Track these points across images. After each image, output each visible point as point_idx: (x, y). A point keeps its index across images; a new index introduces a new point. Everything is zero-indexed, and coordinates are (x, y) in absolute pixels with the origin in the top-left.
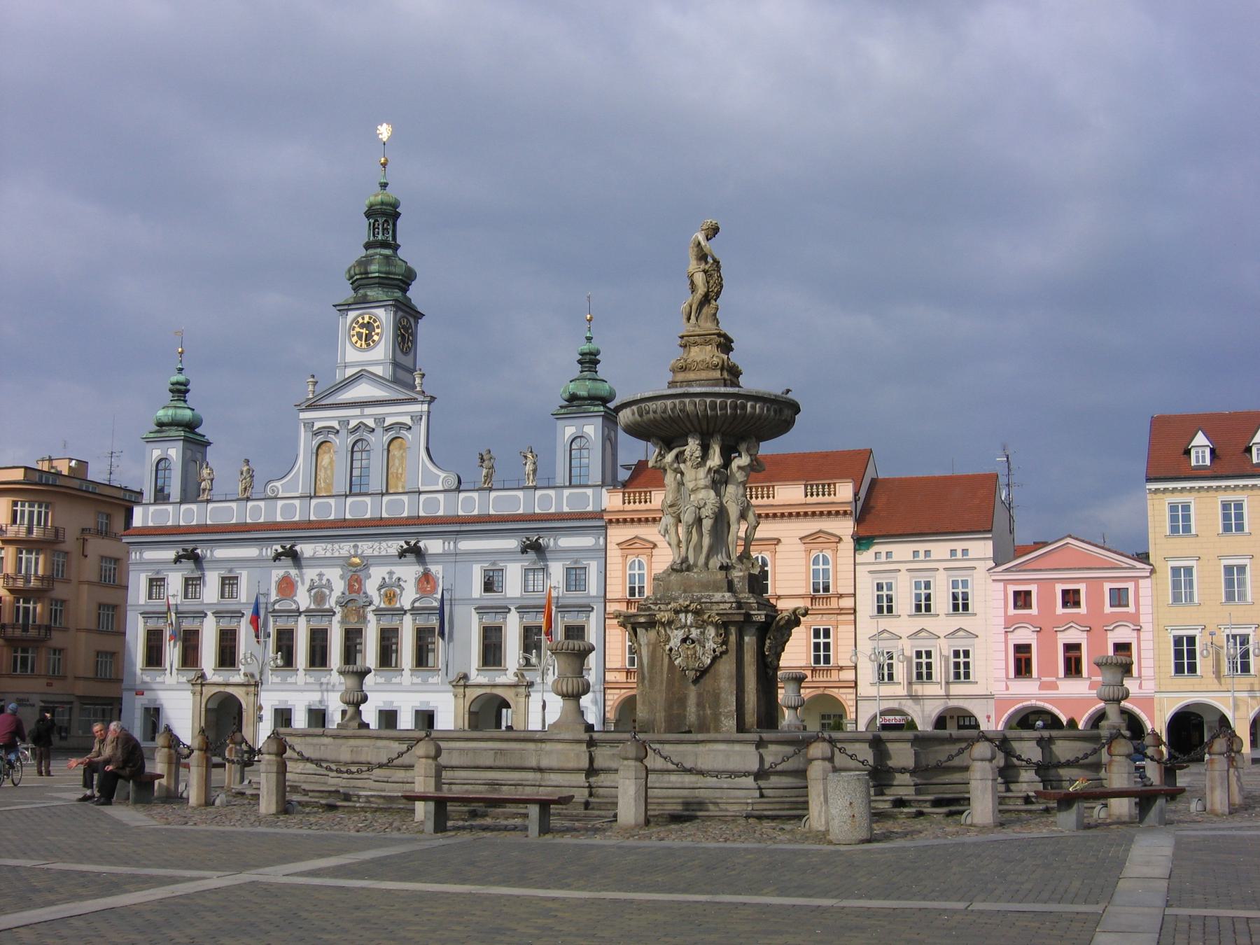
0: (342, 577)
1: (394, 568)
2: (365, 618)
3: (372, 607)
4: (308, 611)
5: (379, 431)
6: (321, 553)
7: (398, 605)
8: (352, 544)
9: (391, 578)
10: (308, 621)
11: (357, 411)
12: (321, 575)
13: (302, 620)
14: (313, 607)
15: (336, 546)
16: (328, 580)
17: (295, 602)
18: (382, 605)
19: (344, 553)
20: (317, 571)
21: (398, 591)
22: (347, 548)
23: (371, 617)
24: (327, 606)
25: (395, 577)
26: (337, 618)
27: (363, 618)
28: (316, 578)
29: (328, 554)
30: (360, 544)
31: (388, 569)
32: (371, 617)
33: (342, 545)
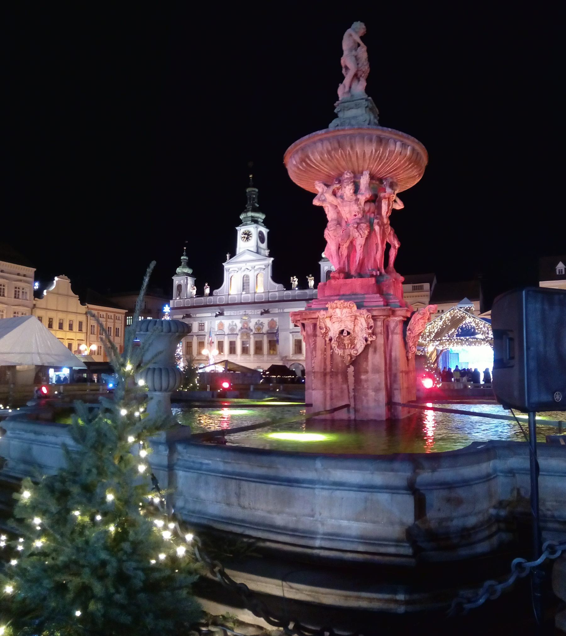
0: (241, 322)
1: (259, 319)
2: (249, 337)
3: (252, 333)
4: (228, 334)
5: (253, 271)
6: (233, 314)
7: (261, 332)
8: (244, 311)
9: (259, 322)
10: (228, 338)
11: (244, 264)
12: (233, 322)
13: (226, 337)
14: (230, 333)
15: (238, 312)
16: (235, 323)
17: (224, 331)
18: (256, 332)
19: (241, 314)
20: (232, 320)
21: (261, 327)
22: (242, 312)
23: (252, 337)
24: (235, 333)
25: (261, 322)
26: (239, 337)
27: (249, 337)
28: (231, 323)
29: (235, 314)
30: (247, 311)
31: (258, 319)
32: (252, 337)
33: (240, 311)
